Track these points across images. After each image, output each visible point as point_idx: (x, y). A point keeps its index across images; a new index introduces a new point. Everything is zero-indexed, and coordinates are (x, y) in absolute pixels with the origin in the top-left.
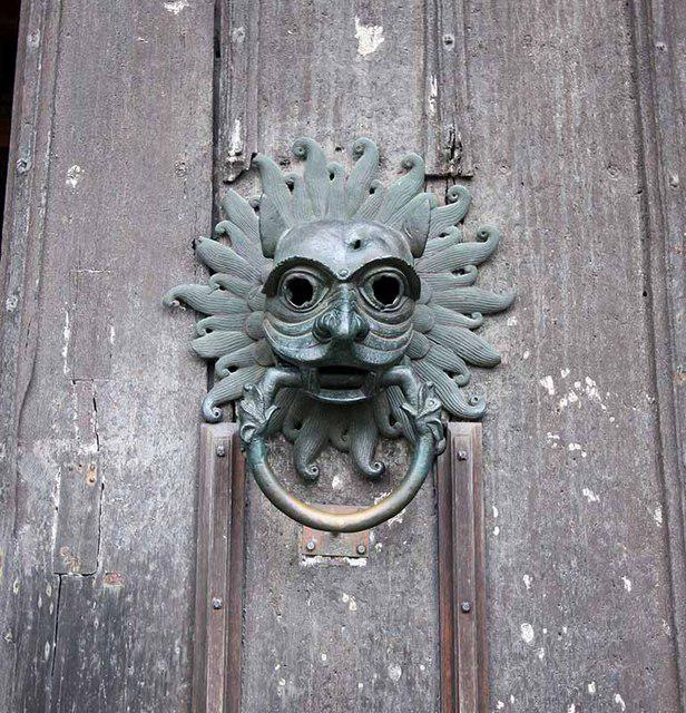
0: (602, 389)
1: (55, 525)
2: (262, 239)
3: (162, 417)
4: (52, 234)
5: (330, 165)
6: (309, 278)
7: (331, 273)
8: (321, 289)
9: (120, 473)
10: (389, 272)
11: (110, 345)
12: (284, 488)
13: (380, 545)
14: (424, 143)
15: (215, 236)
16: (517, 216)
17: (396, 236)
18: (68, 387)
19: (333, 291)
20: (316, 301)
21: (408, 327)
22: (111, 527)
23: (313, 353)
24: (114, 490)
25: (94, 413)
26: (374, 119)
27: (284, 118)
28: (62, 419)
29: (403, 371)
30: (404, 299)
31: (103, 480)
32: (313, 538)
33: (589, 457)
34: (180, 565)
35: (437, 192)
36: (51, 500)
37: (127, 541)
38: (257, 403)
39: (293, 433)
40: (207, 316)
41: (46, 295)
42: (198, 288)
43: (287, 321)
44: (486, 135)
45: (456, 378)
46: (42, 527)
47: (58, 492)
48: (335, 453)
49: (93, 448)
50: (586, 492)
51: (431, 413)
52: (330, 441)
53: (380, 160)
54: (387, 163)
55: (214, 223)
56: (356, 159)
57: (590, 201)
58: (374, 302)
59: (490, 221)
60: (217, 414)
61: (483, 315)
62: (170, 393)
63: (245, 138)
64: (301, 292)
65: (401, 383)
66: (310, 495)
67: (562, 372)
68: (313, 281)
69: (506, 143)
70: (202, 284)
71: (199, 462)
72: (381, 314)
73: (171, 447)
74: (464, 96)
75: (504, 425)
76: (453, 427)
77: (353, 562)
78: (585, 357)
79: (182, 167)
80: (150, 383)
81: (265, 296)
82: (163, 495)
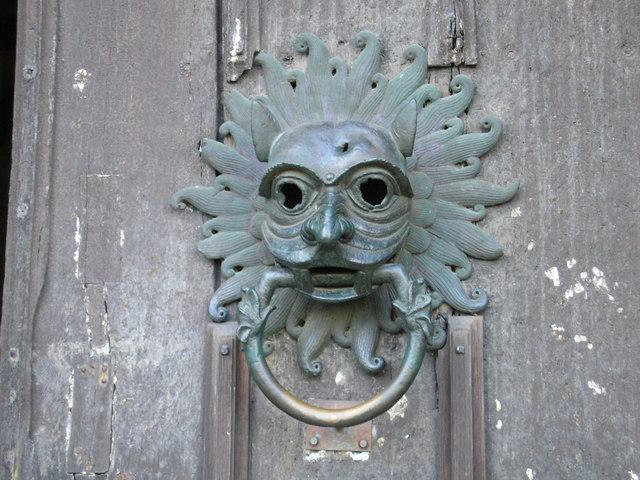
0: (610, 280)
1: (69, 426)
3: (170, 317)
4: (62, 139)
8: (310, 194)
9: (131, 374)
10: (375, 173)
11: (120, 249)
13: (382, 439)
14: (427, 30)
15: (219, 138)
16: (524, 103)
17: (383, 137)
18: (80, 292)
19: (322, 193)
21: (400, 225)
22: (123, 426)
23: (303, 255)
24: (125, 391)
25: (106, 316)
26: (377, 9)
27: (286, 13)
28: (76, 322)
29: (397, 271)
30: (394, 198)
31: (115, 380)
32: (313, 435)
33: (595, 349)
34: (188, 461)
35: (438, 83)
36: (65, 401)
37: (138, 440)
39: (296, 330)
41: (57, 201)
42: (203, 189)
43: (282, 224)
44: (493, 20)
45: (458, 271)
46: (57, 426)
47: (72, 394)
48: (337, 349)
49: (105, 350)
50: (592, 384)
51: (420, 310)
52: (332, 337)
55: (220, 120)
57: (601, 83)
59: (495, 109)
60: (222, 314)
62: (178, 294)
63: (247, 37)
64: (292, 196)
65: (391, 281)
67: (568, 262)
68: (302, 186)
69: (513, 26)
70: (208, 186)
71: (207, 360)
72: (371, 215)
73: (180, 347)
75: (507, 318)
76: (453, 320)
77: (356, 457)
78: (592, 246)
80: (159, 286)
81: (263, 199)
82: (173, 394)
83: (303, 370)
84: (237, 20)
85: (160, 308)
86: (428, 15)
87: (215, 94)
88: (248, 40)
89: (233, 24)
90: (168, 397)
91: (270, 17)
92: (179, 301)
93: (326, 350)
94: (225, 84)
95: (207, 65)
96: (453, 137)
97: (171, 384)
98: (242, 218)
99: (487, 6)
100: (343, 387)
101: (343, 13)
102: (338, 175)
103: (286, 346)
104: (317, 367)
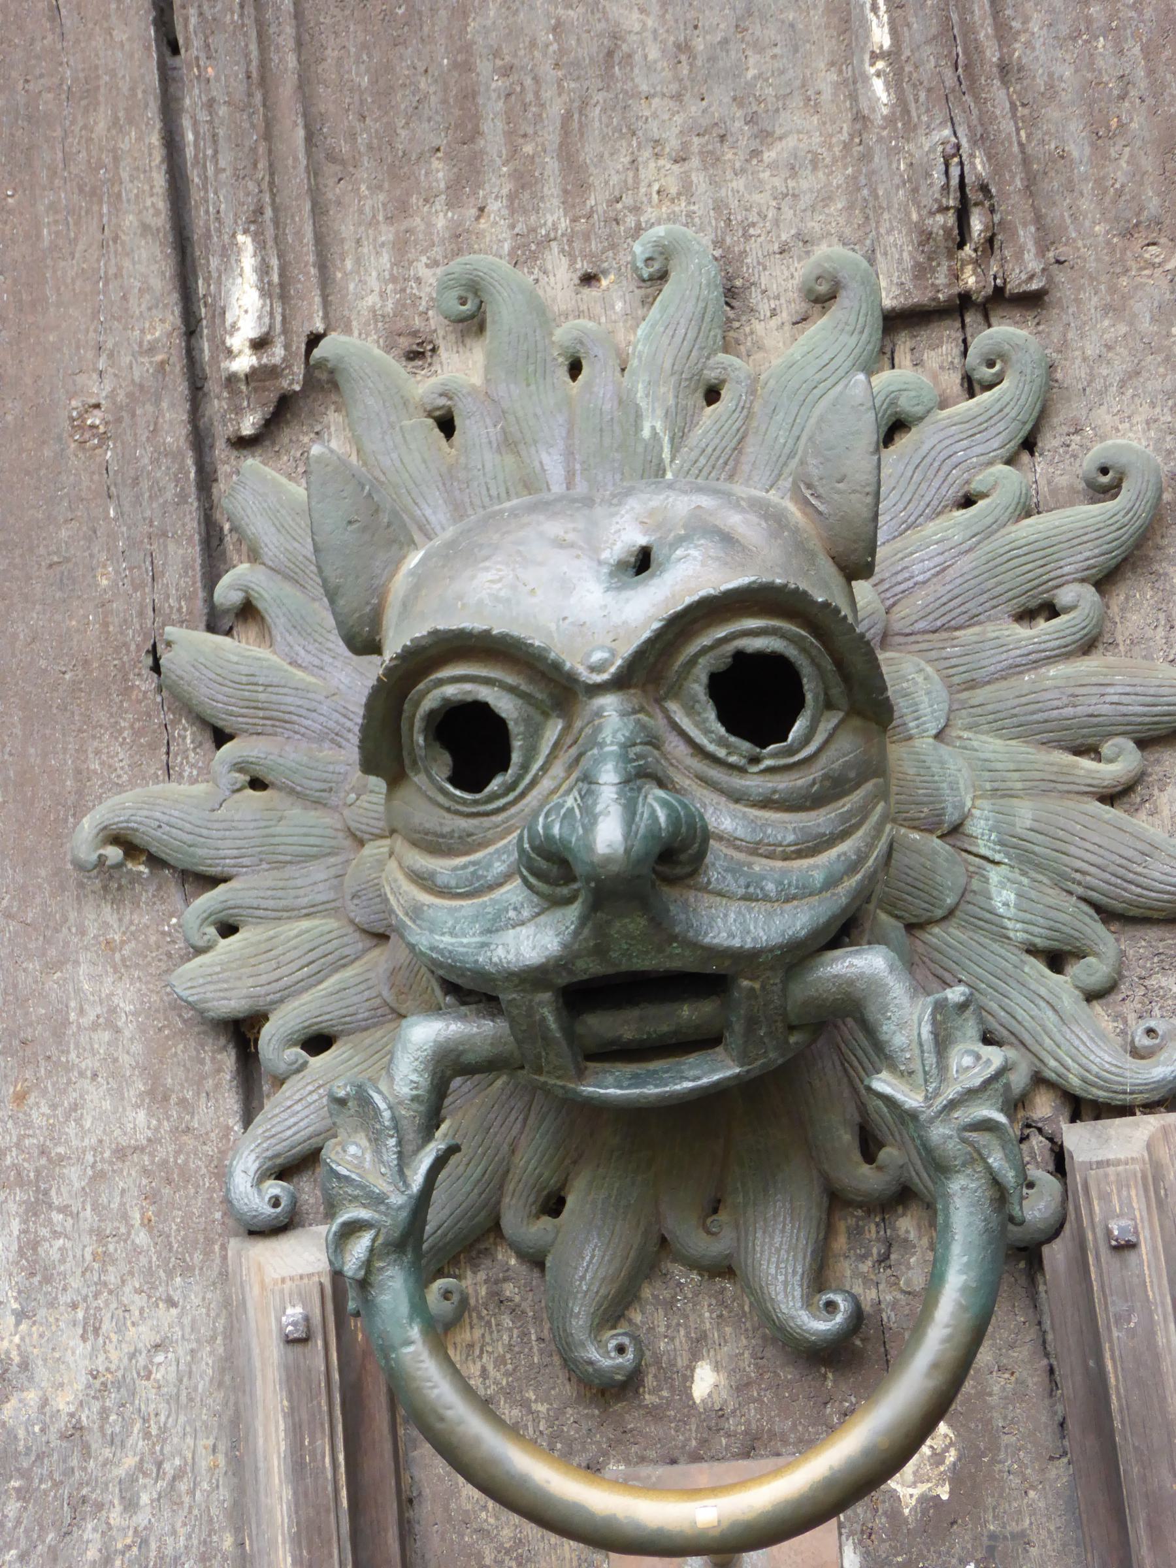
2: (332, 595)
3: (101, 1236)
5: (563, 334)
6: (485, 694)
7: (557, 666)
8: (534, 734)
12: (513, 1431)
20: (525, 767)
21: (863, 813)
26: (695, 162)
27: (400, 210)
38: (376, 1140)
39: (539, 1230)
40: (213, 881)
43: (450, 852)
44: (1078, 149)
45: (1075, 969)
51: (971, 1095)
52: (663, 1241)
53: (731, 294)
54: (755, 297)
56: (647, 302)
58: (721, 742)
60: (276, 1202)
61: (1143, 744)
62: (121, 1153)
66: (621, 1441)
68: (504, 705)
70: (193, 781)
72: (754, 783)
73: (143, 1334)
74: (985, 32)
79: (94, 419)
81: (377, 784)
82: (130, 1505)
83: (574, 1368)
84: (241, 238)
85: (64, 1210)
86: (866, 157)
87: (192, 490)
88: (284, 297)
89: (229, 252)
90: (115, 1516)
91: (346, 228)
92: (129, 1179)
93: (646, 1292)
94: (221, 450)
95: (158, 401)
96: (988, 532)
97: (121, 1472)
98: (318, 872)
99: (1052, 113)
100: (721, 1414)
101: (583, 187)
102: (627, 649)
103: (509, 1289)
104: (621, 1350)
